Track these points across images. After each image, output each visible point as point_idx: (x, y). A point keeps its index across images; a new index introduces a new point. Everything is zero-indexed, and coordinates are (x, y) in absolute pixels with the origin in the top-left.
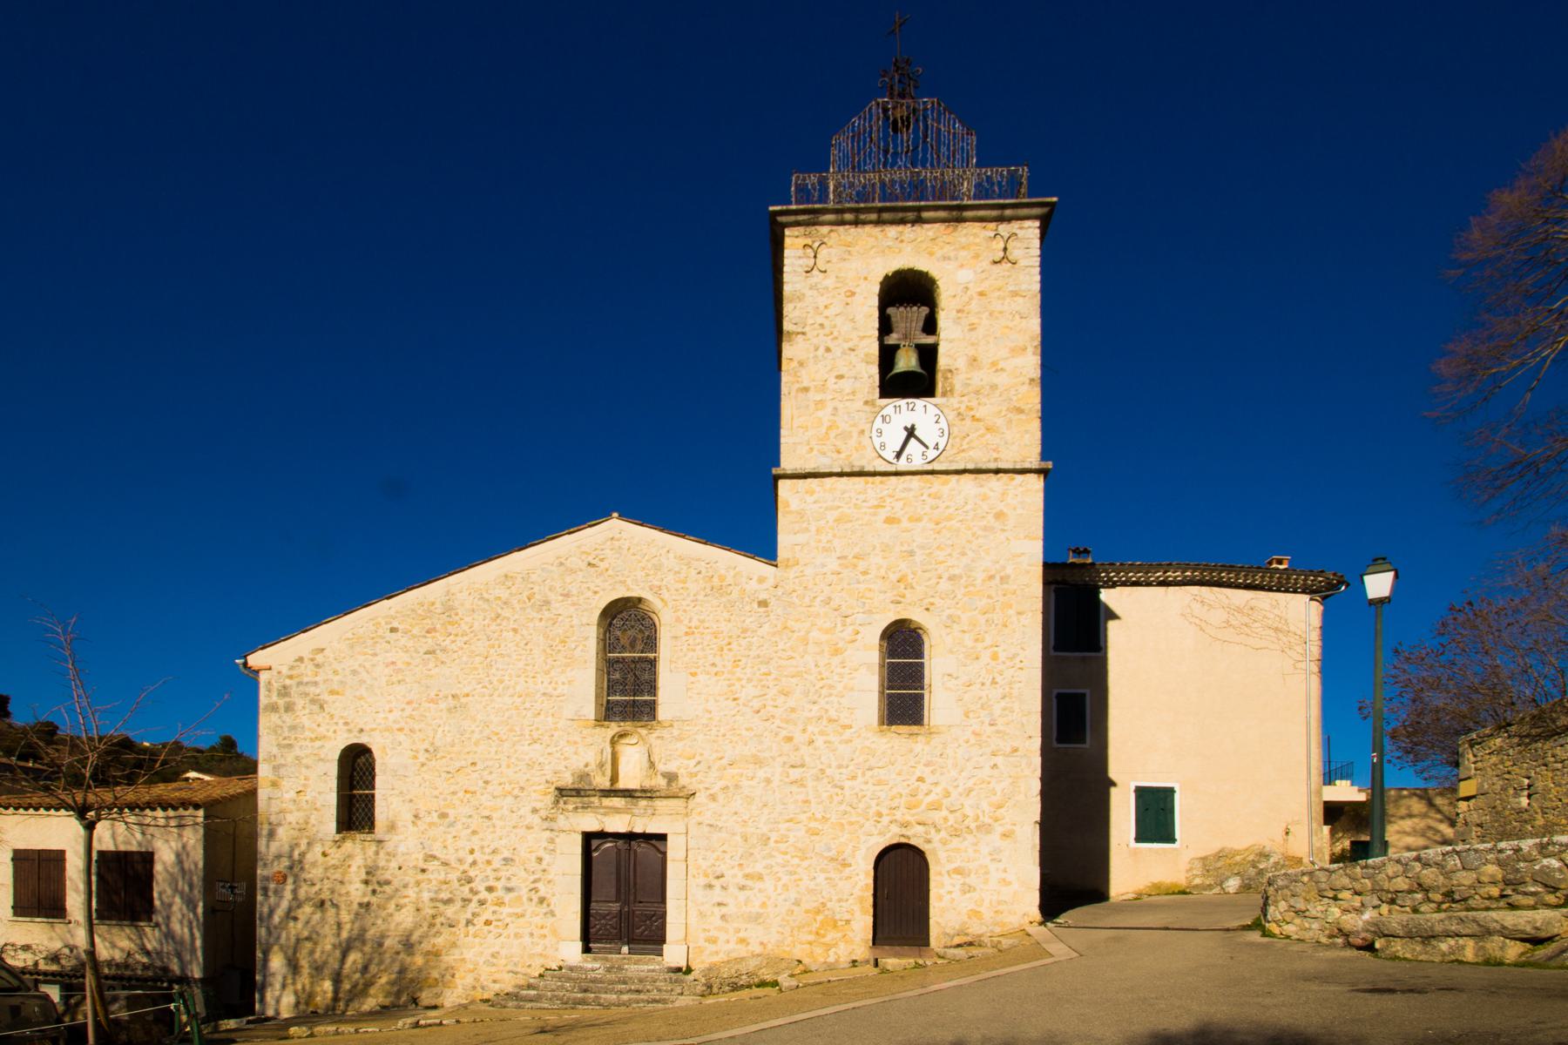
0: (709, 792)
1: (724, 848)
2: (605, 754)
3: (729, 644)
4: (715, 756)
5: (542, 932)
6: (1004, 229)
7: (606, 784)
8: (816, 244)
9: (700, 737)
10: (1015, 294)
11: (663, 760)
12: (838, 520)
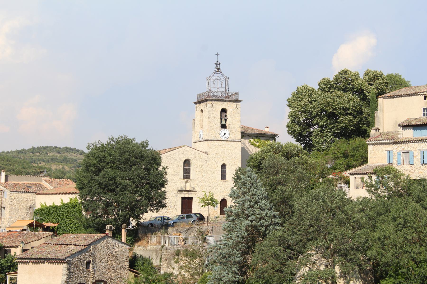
4: (199, 185)
6: (236, 103)
7: (185, 189)
8: (212, 103)
9: (197, 182)
10: (237, 113)
12: (215, 148)
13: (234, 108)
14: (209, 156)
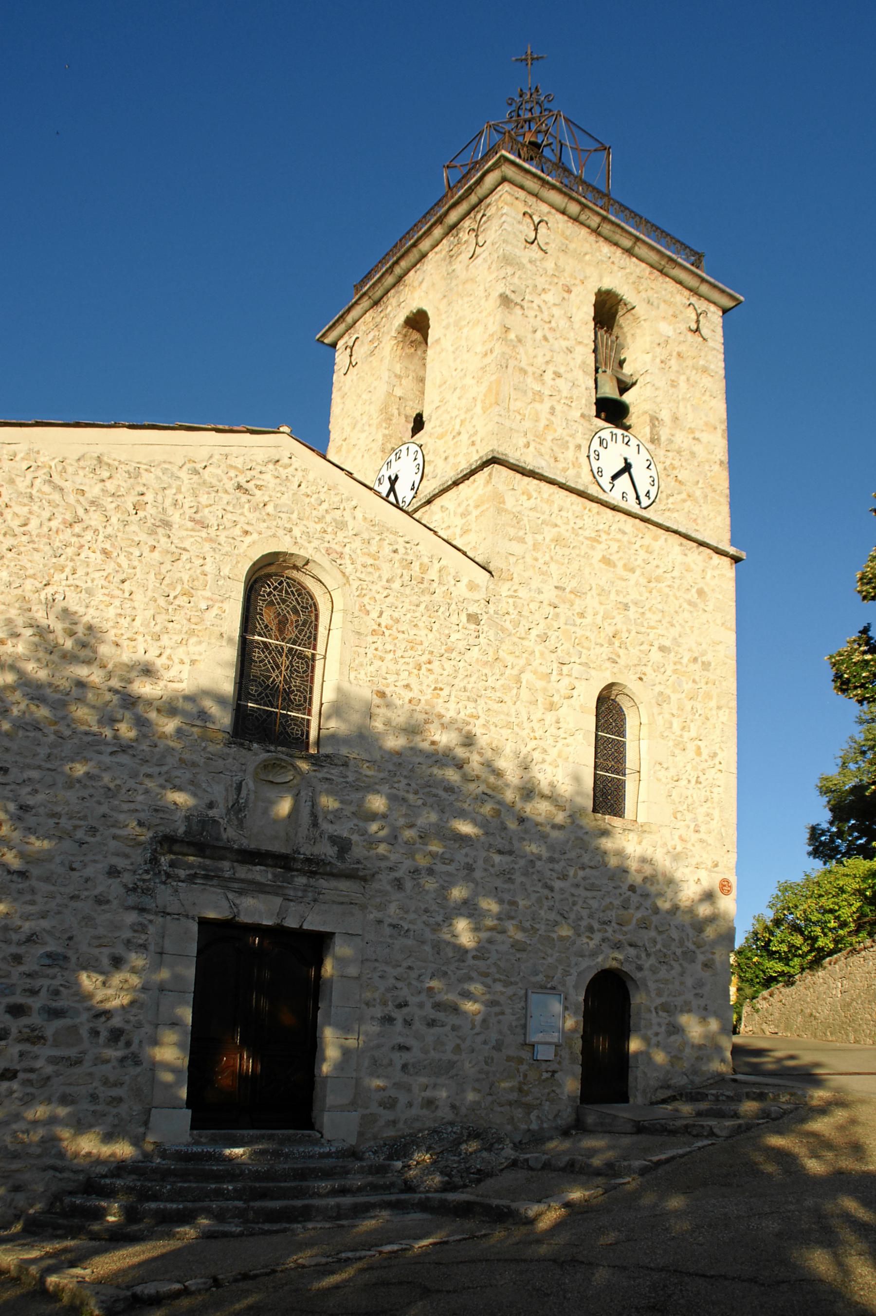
3: (430, 663)
5: (116, 1092)
13: (683, 327)
14: (504, 589)
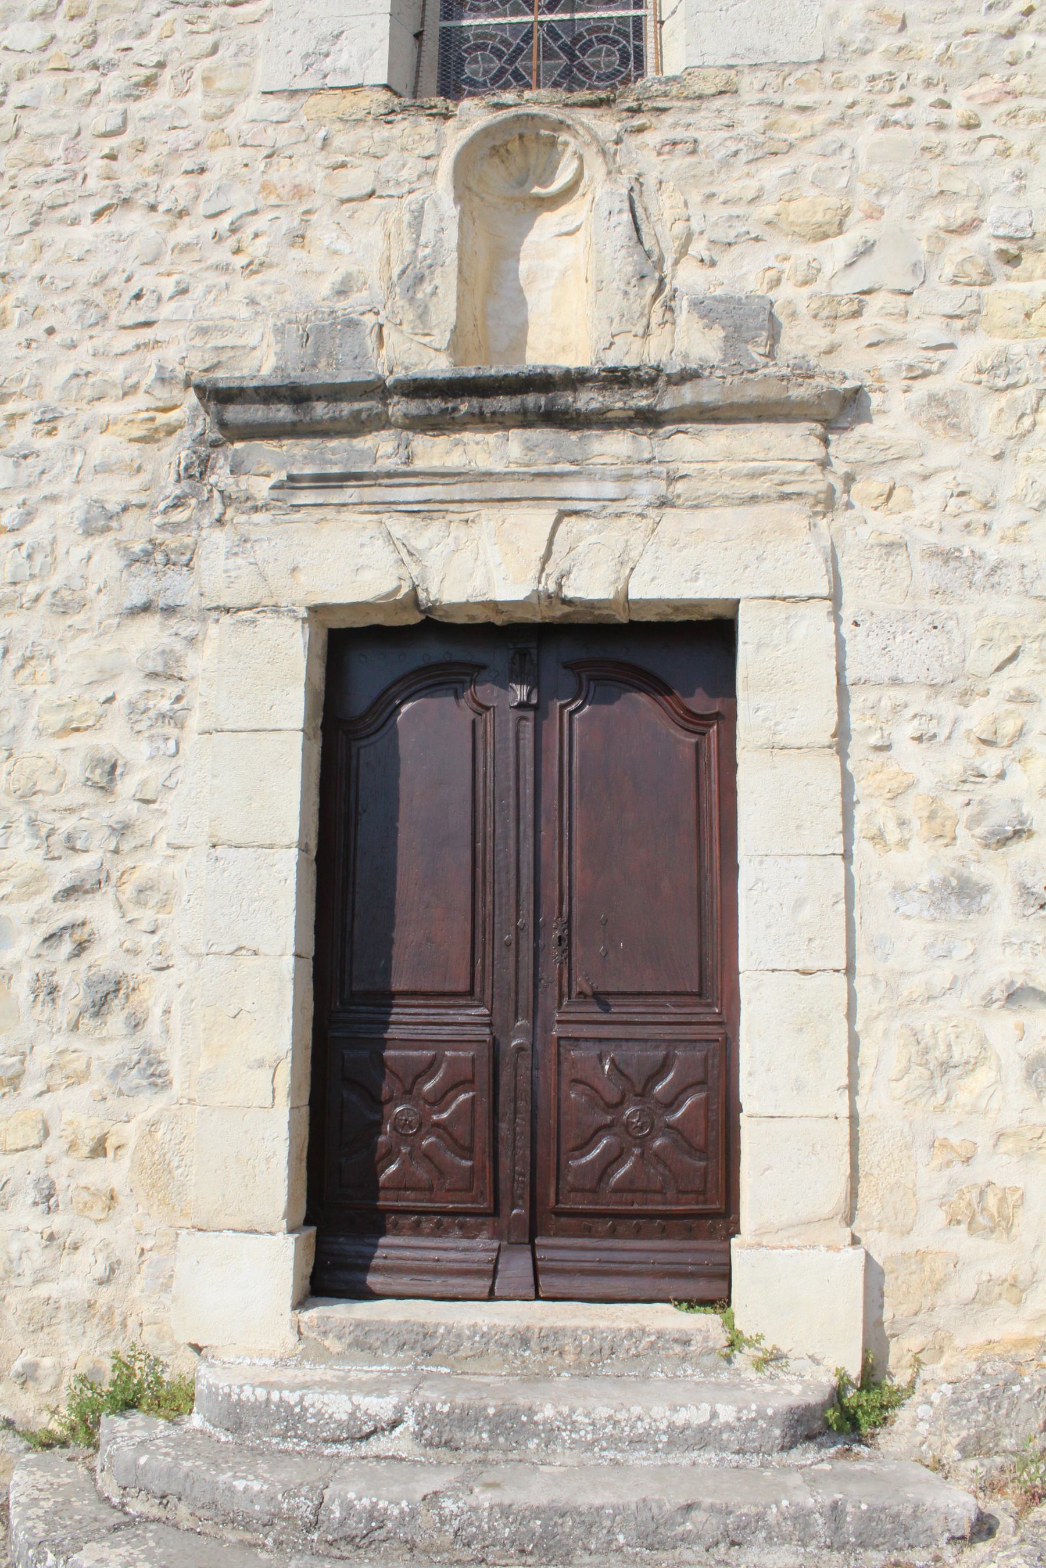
0: (922, 389)
1: (1018, 675)
2: (427, 234)
4: (936, 216)
11: (698, 248)
